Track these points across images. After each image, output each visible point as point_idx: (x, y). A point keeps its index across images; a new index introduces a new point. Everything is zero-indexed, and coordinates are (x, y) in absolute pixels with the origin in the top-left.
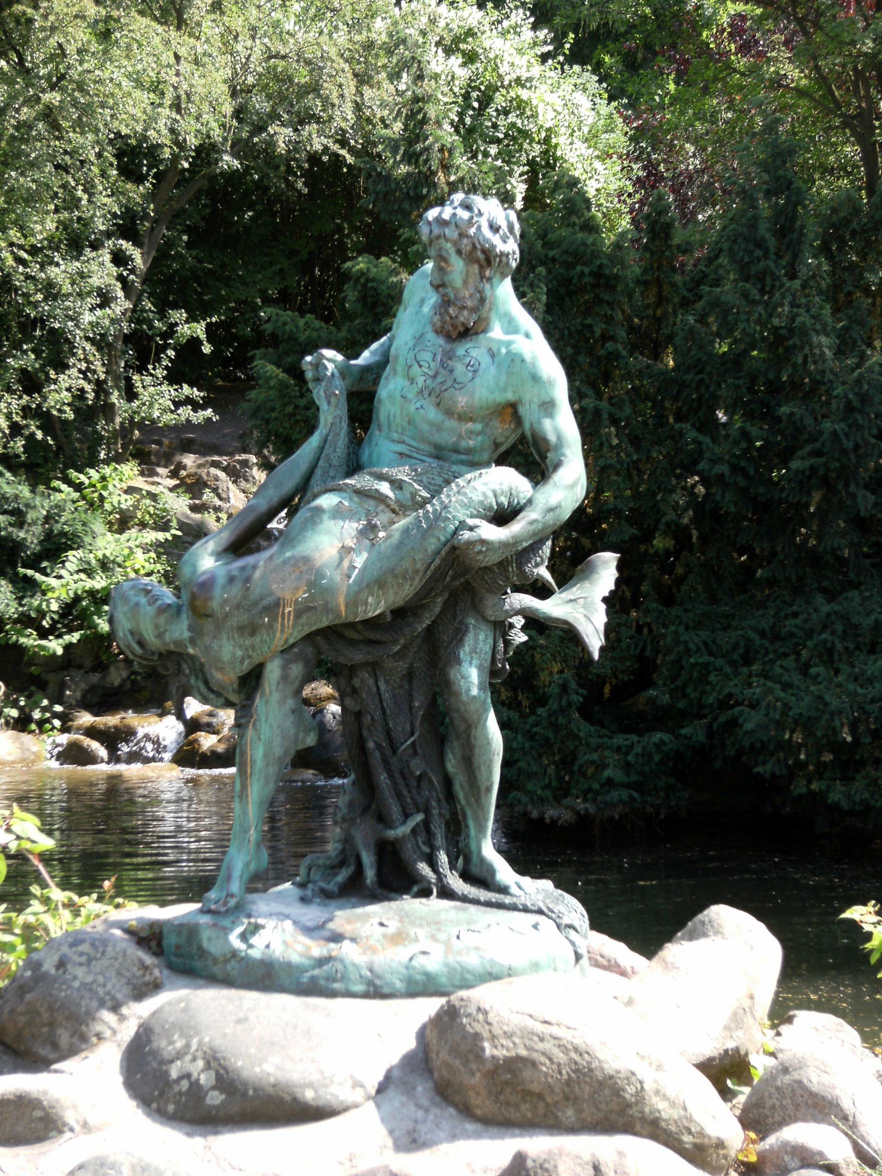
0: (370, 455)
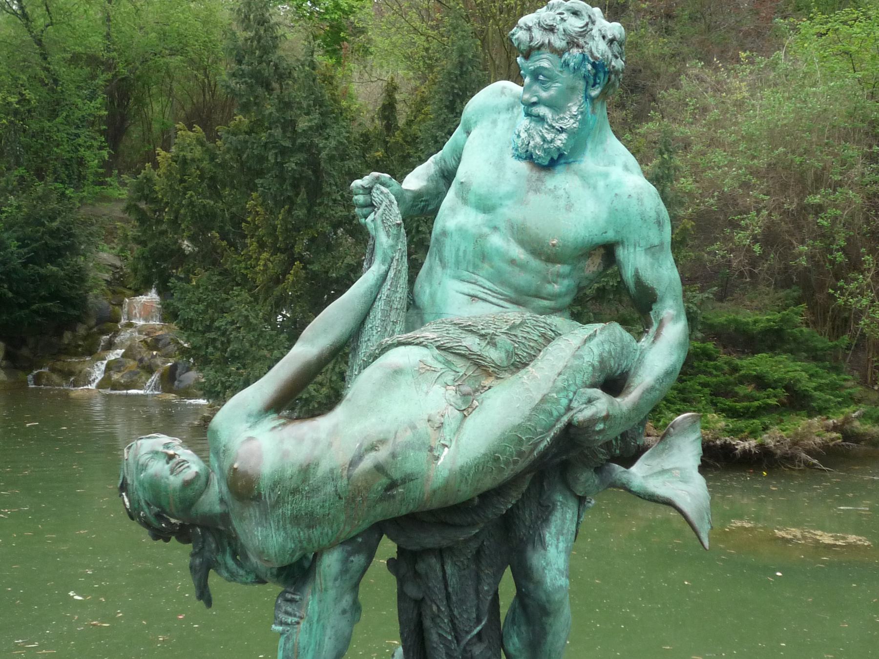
0: (433, 296)
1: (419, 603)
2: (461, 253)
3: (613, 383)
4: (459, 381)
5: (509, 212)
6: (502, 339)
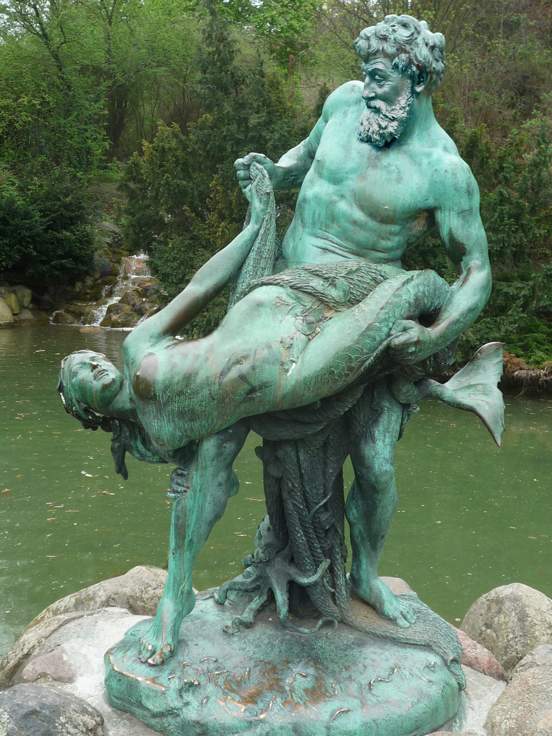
0: (295, 249)
1: (279, 480)
2: (316, 216)
3: (427, 316)
4: (305, 313)
5: (352, 183)
6: (341, 282)
